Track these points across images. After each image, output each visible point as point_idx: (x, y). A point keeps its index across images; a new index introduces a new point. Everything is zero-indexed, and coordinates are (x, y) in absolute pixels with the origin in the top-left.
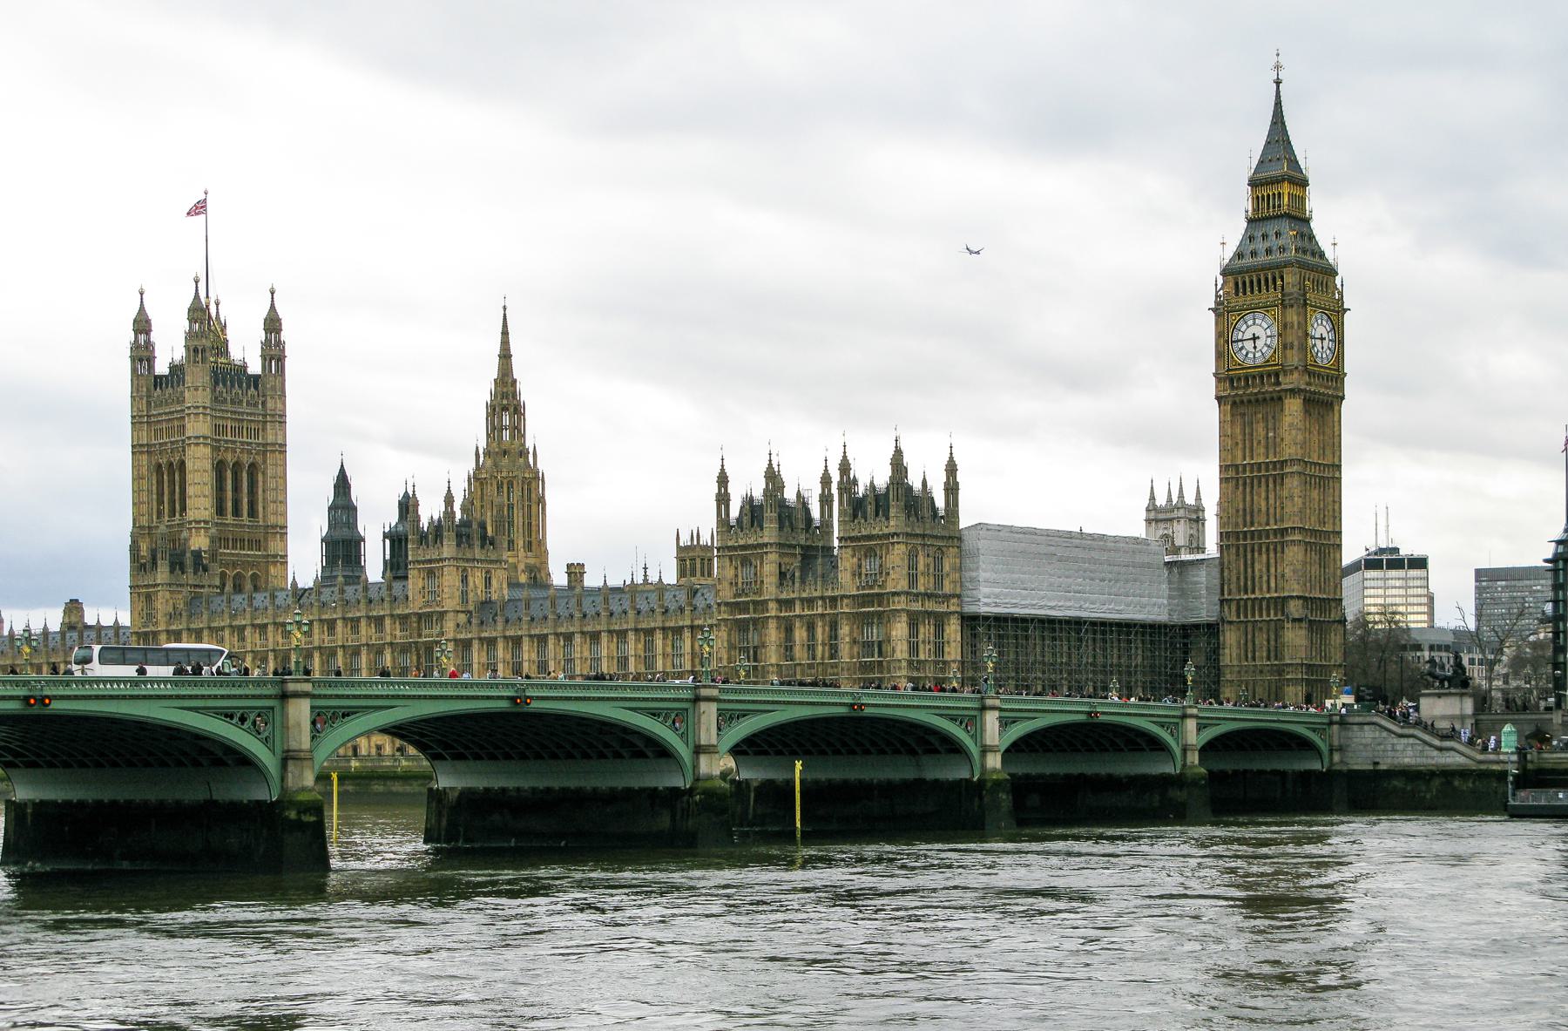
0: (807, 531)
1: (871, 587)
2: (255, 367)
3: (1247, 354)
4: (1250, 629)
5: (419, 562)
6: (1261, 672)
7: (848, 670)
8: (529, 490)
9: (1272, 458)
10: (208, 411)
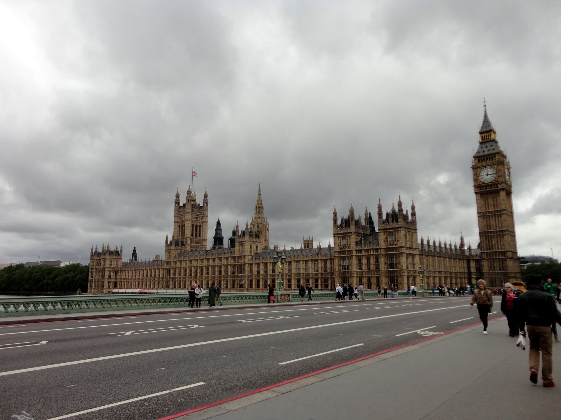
0: (362, 229)
1: (392, 245)
2: (201, 205)
3: (485, 179)
4: (492, 261)
5: (238, 242)
6: (497, 274)
7: (384, 273)
8: (265, 227)
9: (496, 209)
10: (191, 213)
